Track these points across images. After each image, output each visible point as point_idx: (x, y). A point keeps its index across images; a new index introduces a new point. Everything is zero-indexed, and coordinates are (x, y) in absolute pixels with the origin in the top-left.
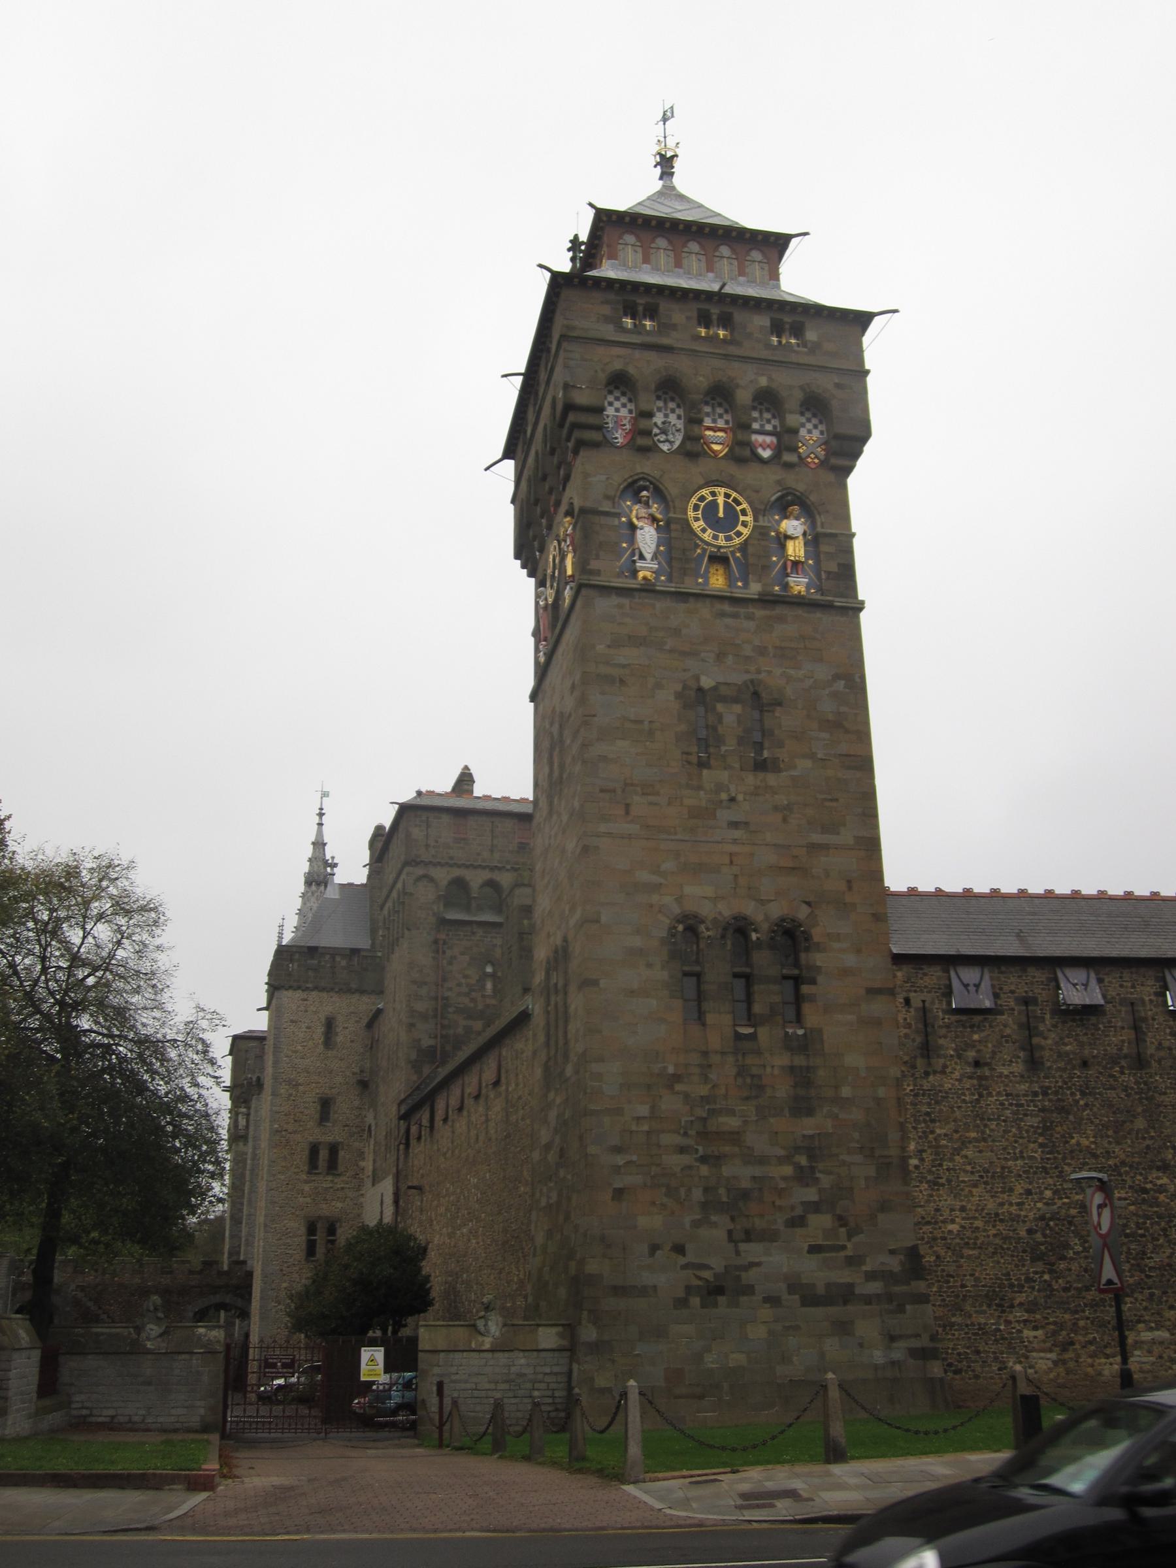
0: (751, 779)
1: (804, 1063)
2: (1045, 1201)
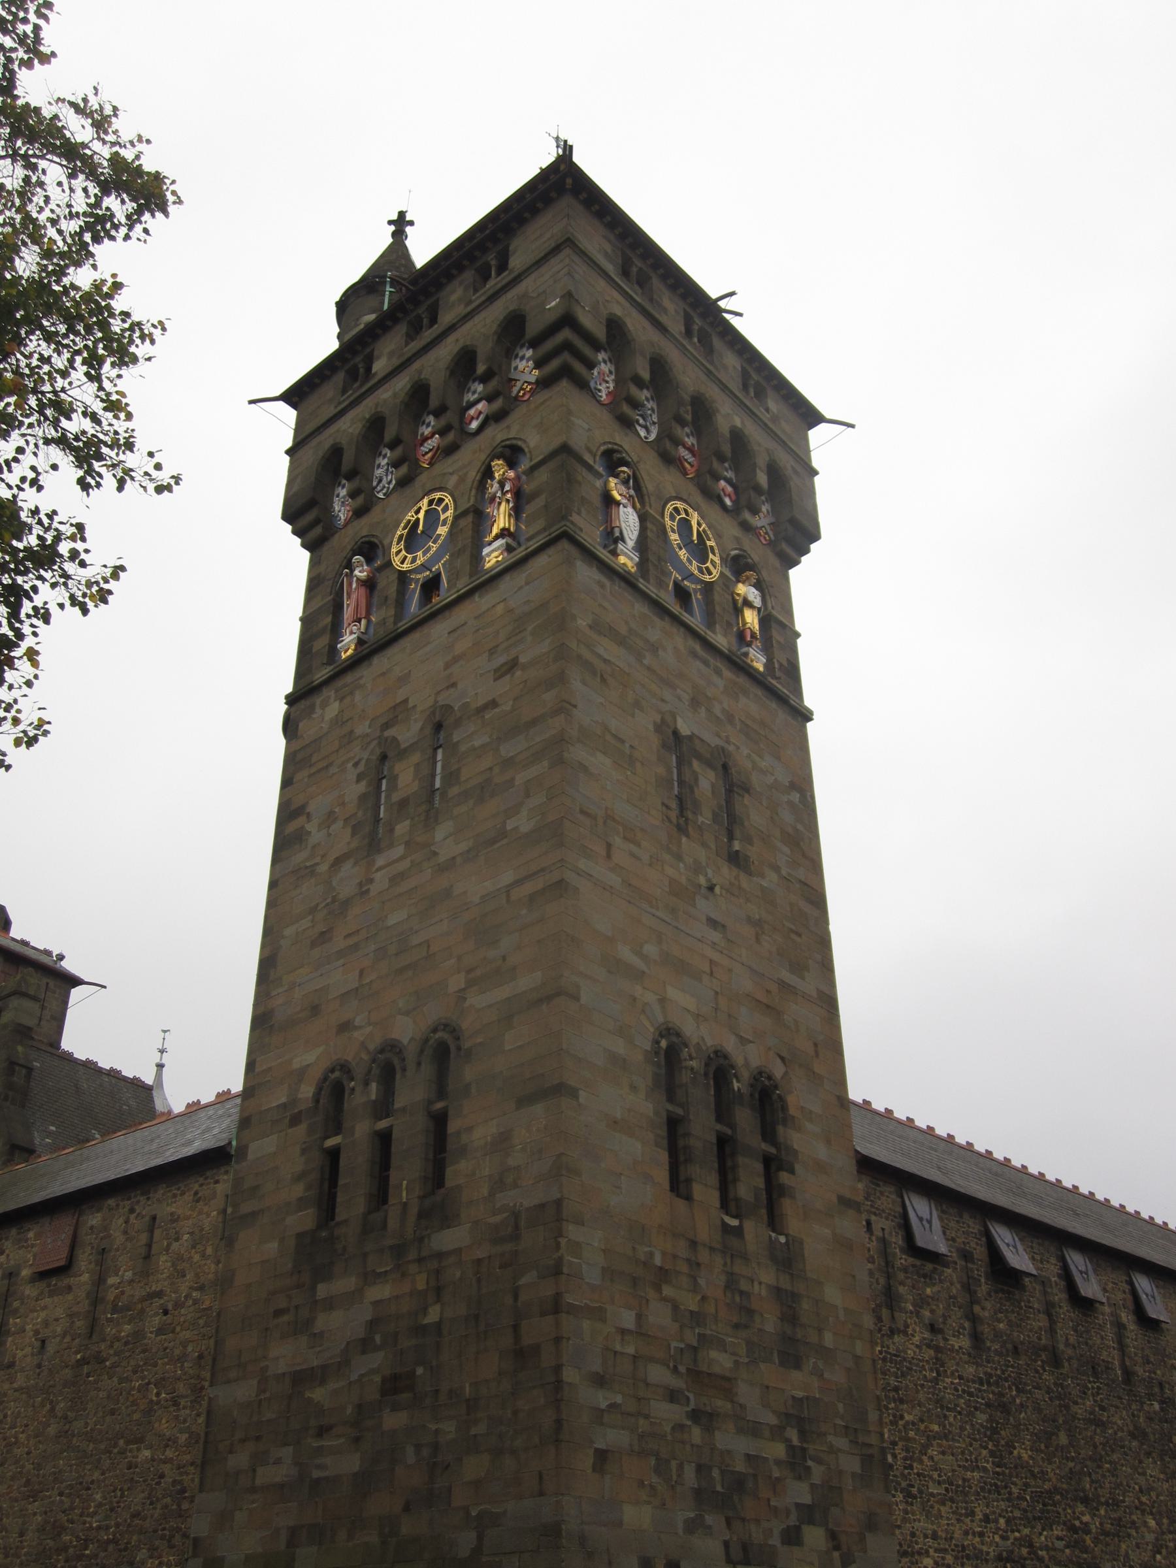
2: (1001, 1533)
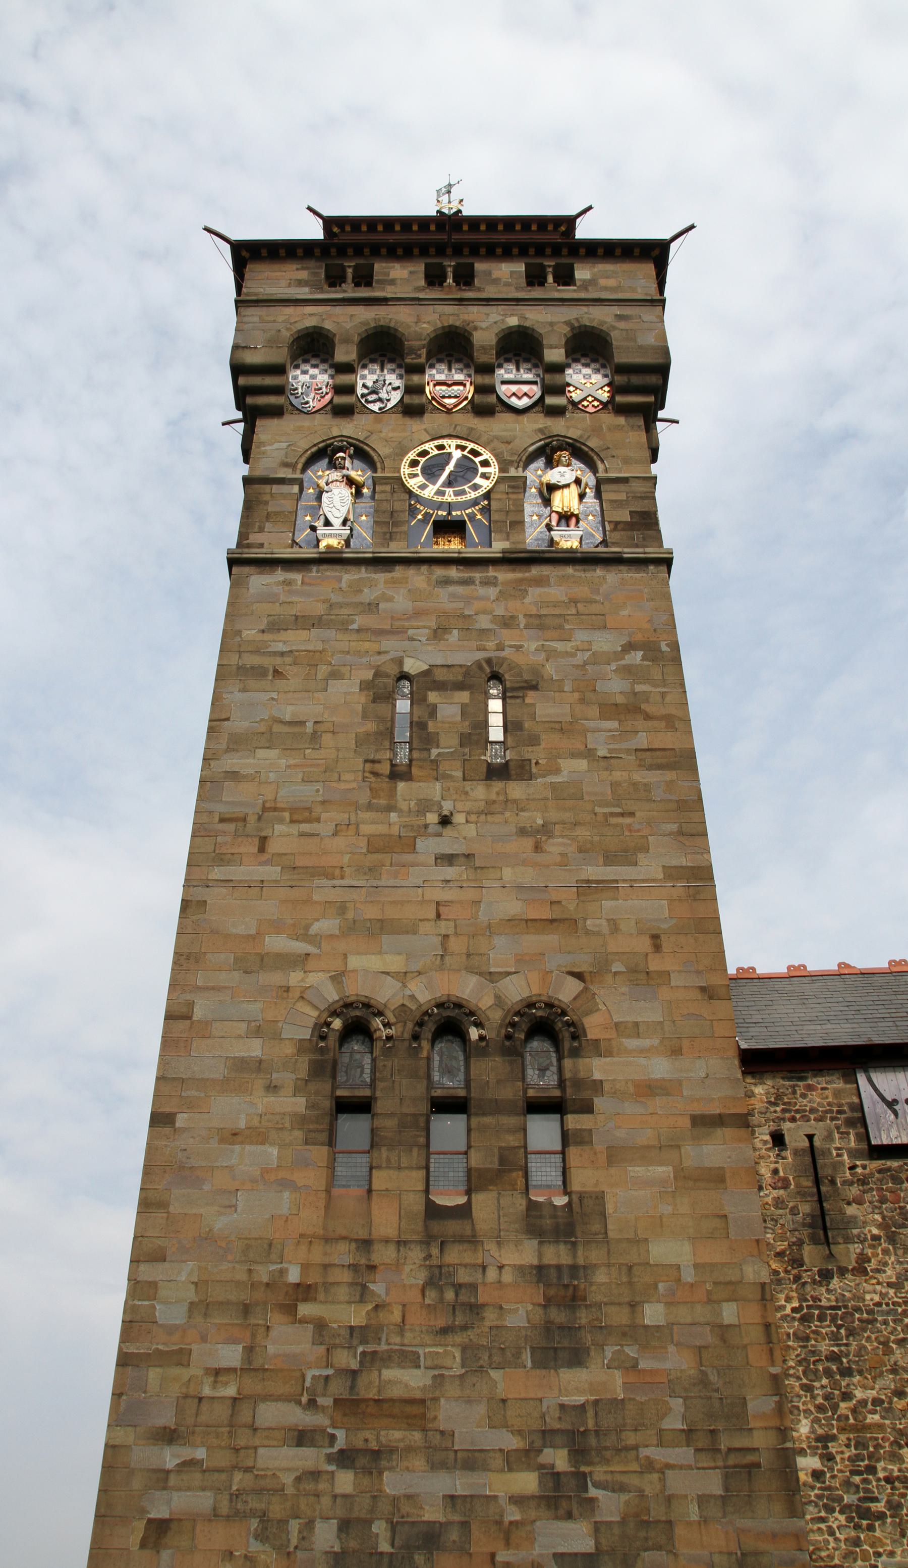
0: (480, 792)
1: (565, 1259)
